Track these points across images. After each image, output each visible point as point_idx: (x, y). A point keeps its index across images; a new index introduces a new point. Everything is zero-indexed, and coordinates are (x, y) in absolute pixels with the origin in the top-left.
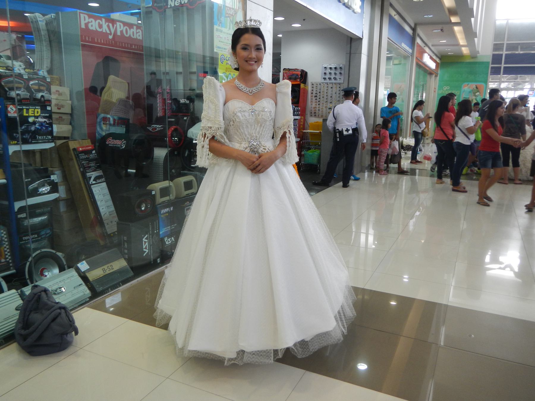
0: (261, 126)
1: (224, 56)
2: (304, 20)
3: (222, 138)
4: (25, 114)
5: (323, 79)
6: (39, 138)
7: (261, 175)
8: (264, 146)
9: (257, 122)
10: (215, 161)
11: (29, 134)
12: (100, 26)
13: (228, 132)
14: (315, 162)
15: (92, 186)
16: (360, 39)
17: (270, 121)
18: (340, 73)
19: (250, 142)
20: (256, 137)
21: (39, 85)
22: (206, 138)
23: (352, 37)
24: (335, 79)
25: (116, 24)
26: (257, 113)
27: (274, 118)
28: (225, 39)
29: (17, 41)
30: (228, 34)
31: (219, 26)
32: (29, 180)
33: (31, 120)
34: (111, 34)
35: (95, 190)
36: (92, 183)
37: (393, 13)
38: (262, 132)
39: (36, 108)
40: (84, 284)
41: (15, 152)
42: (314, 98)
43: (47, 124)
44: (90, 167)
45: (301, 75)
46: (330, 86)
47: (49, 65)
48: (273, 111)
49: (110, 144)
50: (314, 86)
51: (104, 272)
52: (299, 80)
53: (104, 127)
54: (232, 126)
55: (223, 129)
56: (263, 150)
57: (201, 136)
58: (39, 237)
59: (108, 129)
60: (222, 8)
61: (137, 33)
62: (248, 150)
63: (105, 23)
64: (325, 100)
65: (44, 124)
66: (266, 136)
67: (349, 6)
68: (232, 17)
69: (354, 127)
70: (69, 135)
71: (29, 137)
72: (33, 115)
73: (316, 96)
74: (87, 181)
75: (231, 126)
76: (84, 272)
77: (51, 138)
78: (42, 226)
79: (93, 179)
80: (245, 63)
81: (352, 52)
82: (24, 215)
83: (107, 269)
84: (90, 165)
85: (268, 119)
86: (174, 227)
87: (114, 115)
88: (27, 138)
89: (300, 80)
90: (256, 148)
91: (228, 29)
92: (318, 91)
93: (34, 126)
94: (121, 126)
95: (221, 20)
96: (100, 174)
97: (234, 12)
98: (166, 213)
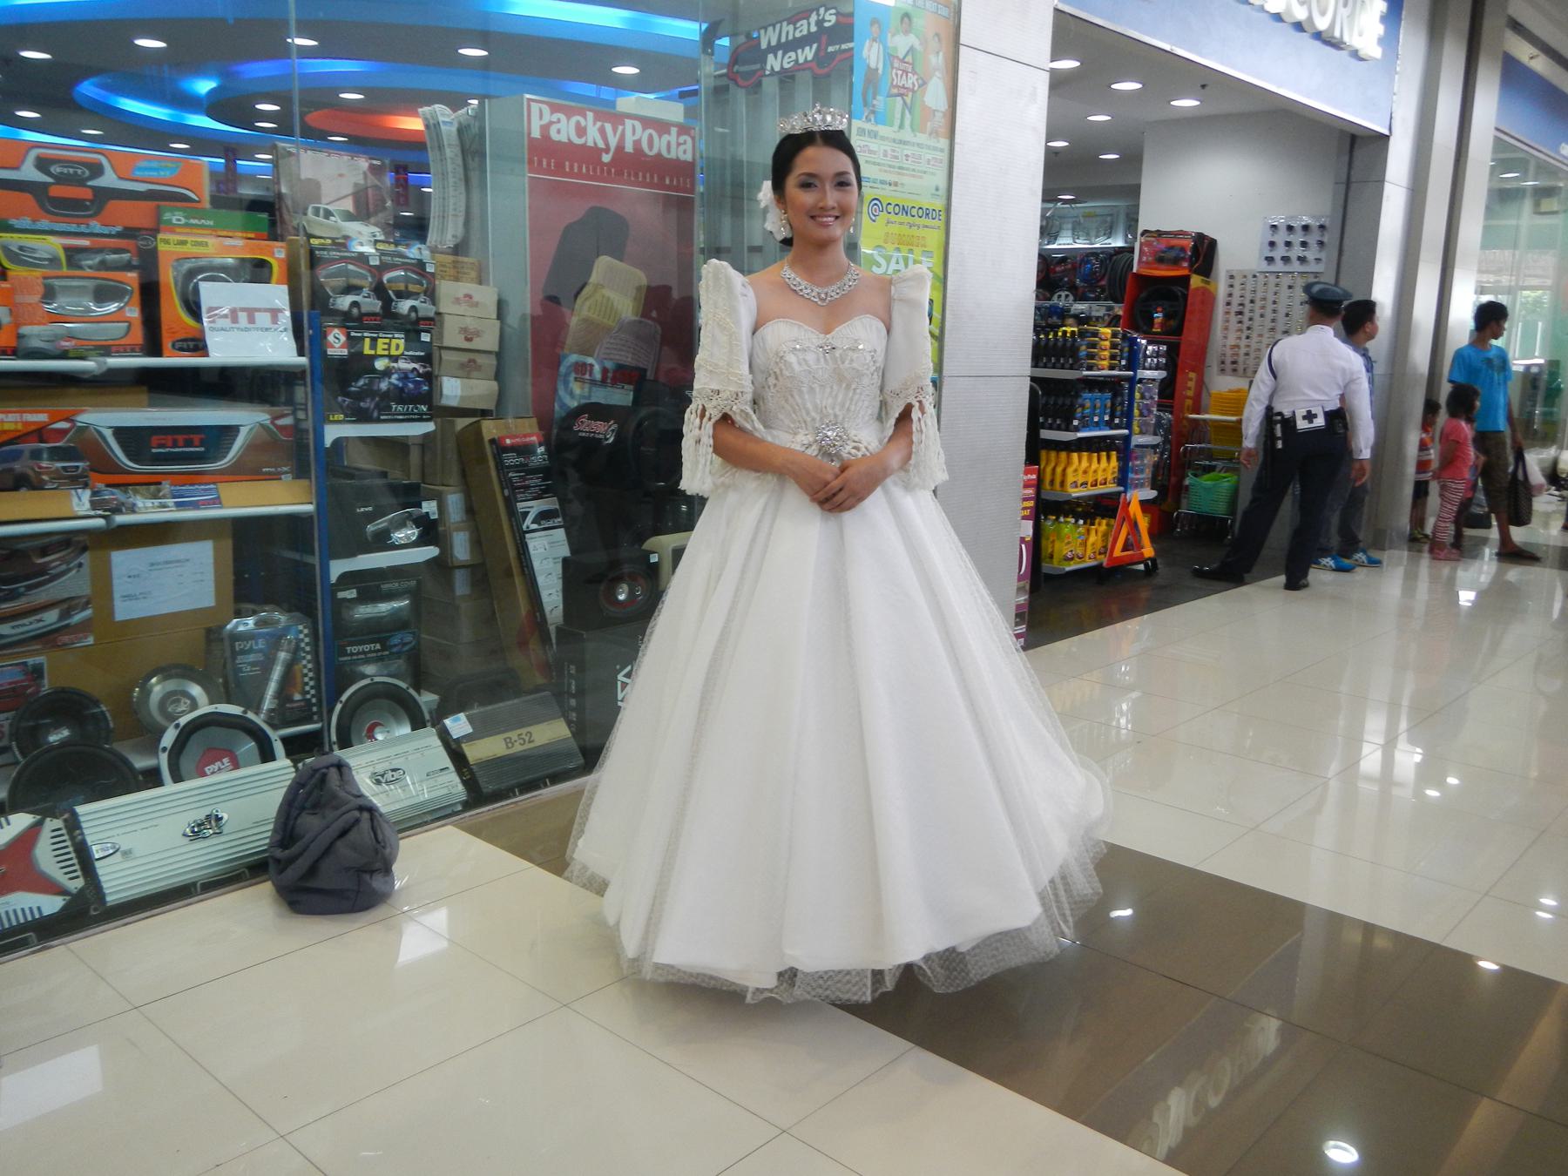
0: (848, 387)
1: (880, 202)
2: (1203, 86)
3: (746, 420)
4: (367, 351)
5: (1266, 262)
6: (396, 408)
7: (847, 516)
8: (854, 442)
9: (839, 377)
10: (726, 479)
11: (373, 399)
12: (581, 131)
13: (763, 402)
14: (1220, 509)
15: (527, 535)
16: (1381, 141)
17: (872, 375)
18: (1321, 243)
19: (817, 431)
20: (836, 416)
21: (407, 280)
22: (705, 419)
23: (1353, 131)
24: (1302, 260)
25: (623, 124)
26: (837, 355)
27: (882, 367)
28: (885, 155)
29: (369, 174)
30: (894, 141)
31: (868, 120)
32: (370, 509)
33: (380, 365)
34: (607, 150)
35: (535, 547)
36: (528, 528)
37: (1524, 52)
38: (851, 404)
39: (394, 338)
40: (452, 768)
41: (338, 443)
42: (1233, 319)
43: (419, 375)
44: (527, 487)
45: (1195, 249)
46: (1286, 281)
47: (460, 232)
48: (881, 349)
49: (582, 431)
50: (1237, 283)
51: (508, 748)
52: (1185, 264)
53: (577, 388)
54: (772, 388)
55: (749, 397)
56: (853, 451)
57: (693, 416)
58: (387, 650)
59: (586, 394)
60: (880, 72)
61: (679, 144)
62: (813, 451)
63: (594, 124)
64: (1269, 325)
65: (411, 376)
66: (860, 416)
67: (1334, 41)
68: (910, 94)
69: (1334, 405)
70: (489, 405)
71: (372, 406)
72: (386, 353)
73: (1240, 313)
74: (516, 520)
75: (769, 387)
76: (458, 741)
78: (397, 623)
79: (533, 516)
80: (810, 224)
81: (1353, 179)
82: (352, 593)
83: (515, 741)
84: (527, 483)
85: (867, 369)
87: (606, 359)
88: (367, 409)
89: (1191, 266)
90: (835, 445)
91: (896, 128)
92: (1249, 296)
93: (387, 379)
94: (623, 388)
95: (874, 106)
96: (552, 507)
97: (917, 80)
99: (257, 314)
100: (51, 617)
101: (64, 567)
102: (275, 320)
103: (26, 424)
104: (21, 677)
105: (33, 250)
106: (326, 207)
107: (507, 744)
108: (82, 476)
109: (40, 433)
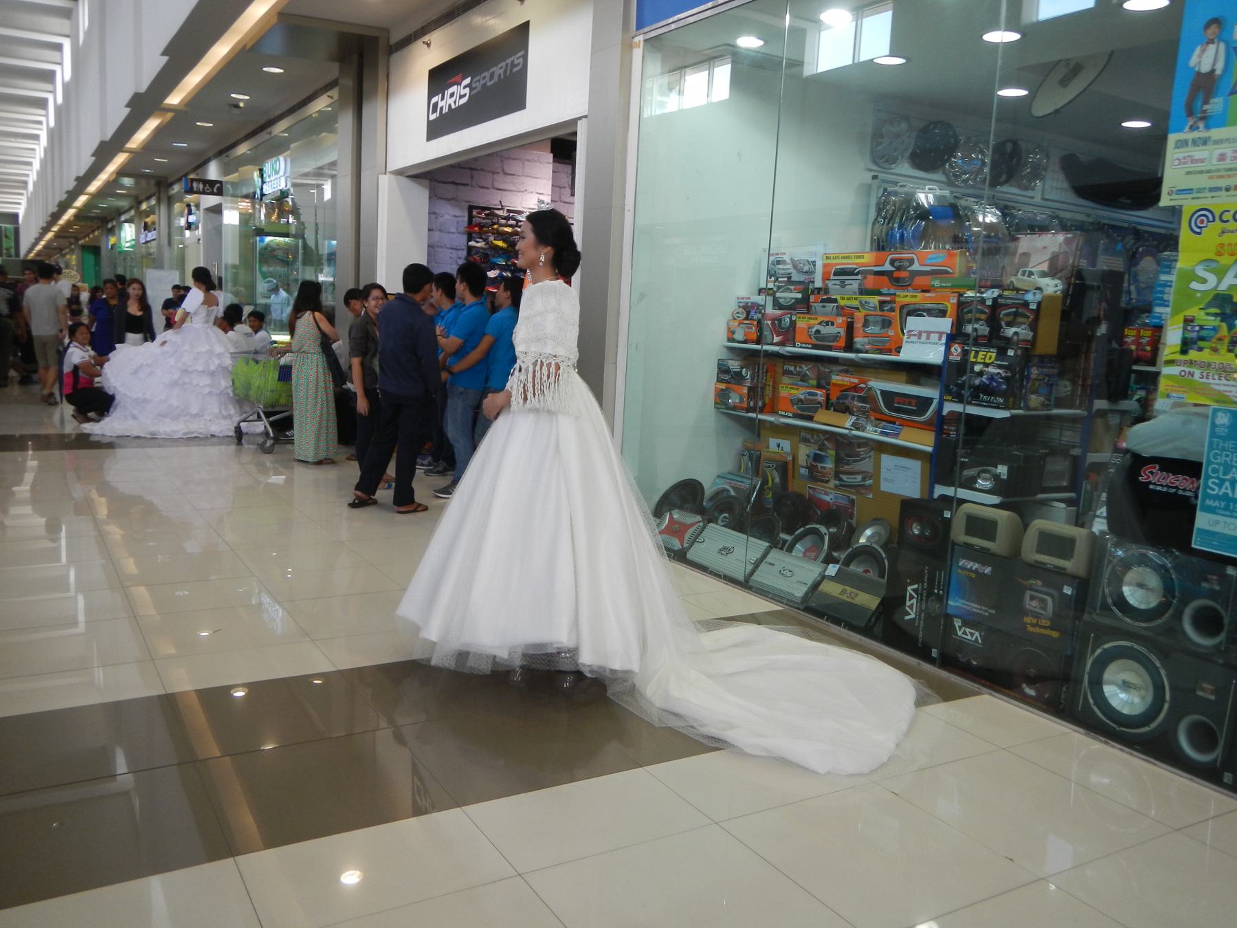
29: (1063, 244)
39: (989, 352)
41: (951, 413)
43: (1002, 378)
65: (995, 377)
72: (982, 361)
77: (1004, 402)
86: (987, 614)
98: (970, 570)
99: (932, 335)
100: (859, 478)
101: (864, 456)
102: (940, 338)
103: (851, 383)
104: (847, 503)
105: (869, 303)
106: (1031, 269)
107: (842, 591)
108: (867, 412)
109: (855, 388)
